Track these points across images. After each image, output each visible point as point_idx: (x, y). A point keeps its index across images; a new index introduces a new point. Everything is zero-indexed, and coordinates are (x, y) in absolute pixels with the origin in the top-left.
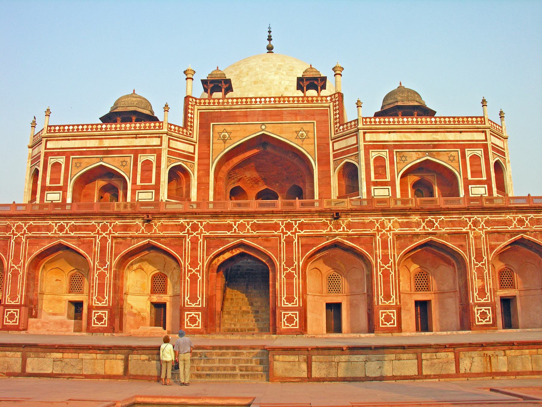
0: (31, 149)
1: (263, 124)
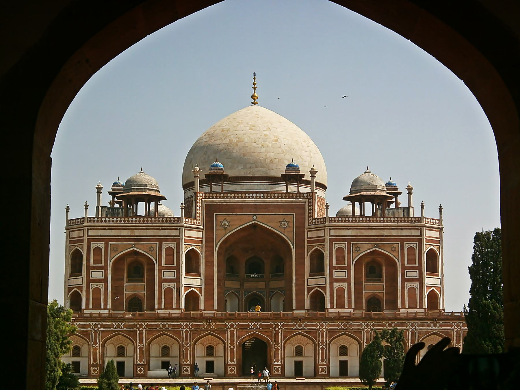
0: (68, 231)
1: (255, 215)
